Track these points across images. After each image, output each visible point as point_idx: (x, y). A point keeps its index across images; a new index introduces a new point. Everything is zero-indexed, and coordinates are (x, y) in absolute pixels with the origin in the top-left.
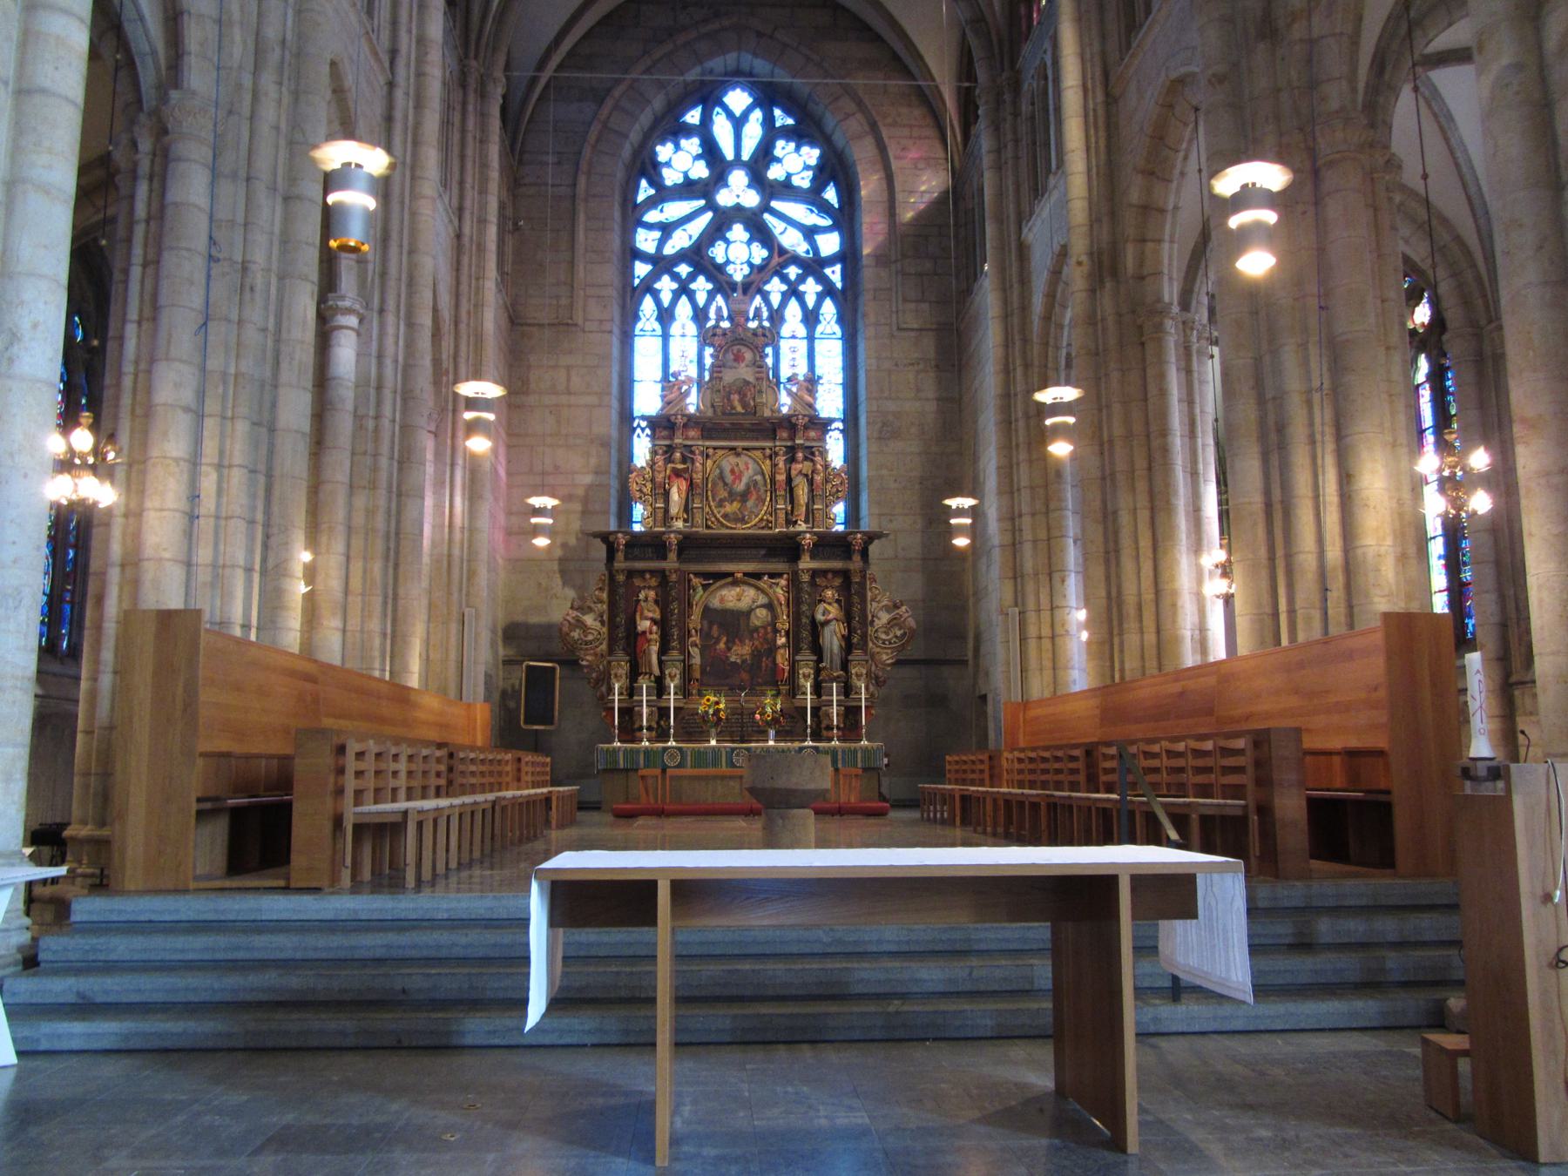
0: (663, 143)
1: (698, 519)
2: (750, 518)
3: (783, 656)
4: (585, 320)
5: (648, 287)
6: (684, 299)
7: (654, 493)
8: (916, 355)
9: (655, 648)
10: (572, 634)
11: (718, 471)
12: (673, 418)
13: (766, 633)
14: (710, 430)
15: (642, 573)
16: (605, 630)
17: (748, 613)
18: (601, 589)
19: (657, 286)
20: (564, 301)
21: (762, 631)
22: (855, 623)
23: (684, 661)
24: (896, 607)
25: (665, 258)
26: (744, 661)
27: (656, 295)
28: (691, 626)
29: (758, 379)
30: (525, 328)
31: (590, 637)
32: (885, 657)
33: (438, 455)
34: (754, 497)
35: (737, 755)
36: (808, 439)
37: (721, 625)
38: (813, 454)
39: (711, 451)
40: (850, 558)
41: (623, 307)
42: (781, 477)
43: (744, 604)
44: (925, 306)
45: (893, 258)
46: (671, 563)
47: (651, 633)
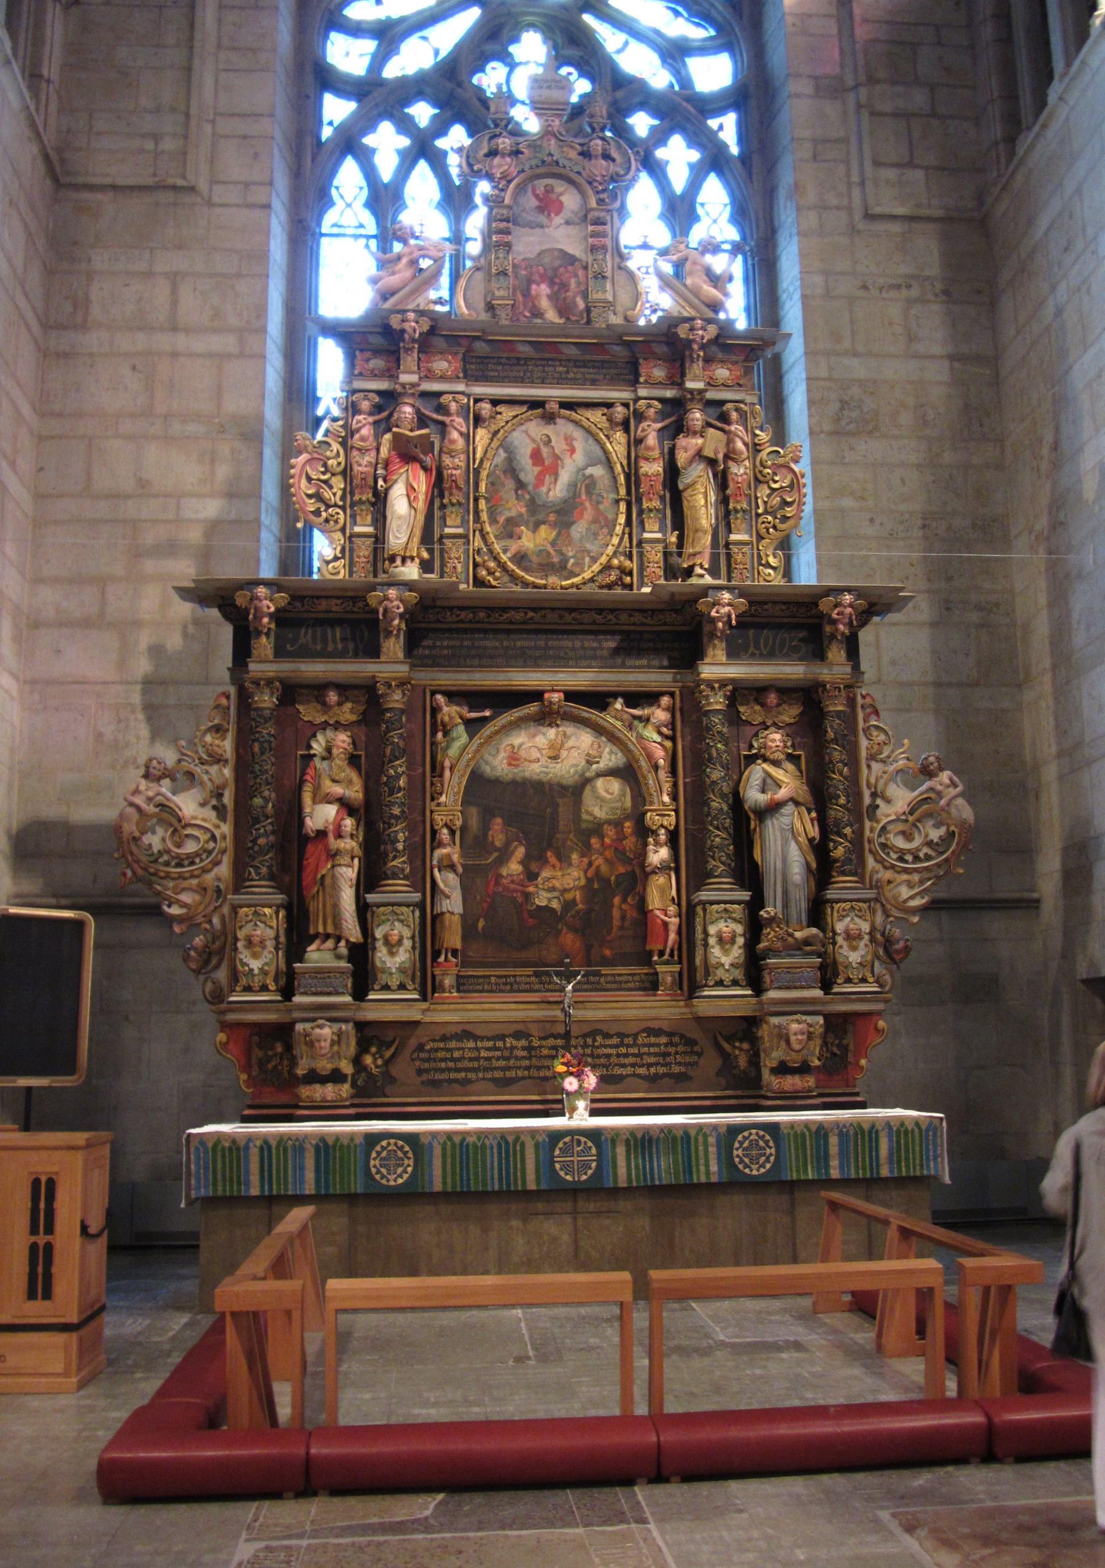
1: (456, 558)
2: (579, 564)
3: (663, 891)
4: (213, 181)
6: (423, 167)
7: (349, 503)
8: (903, 269)
9: (348, 873)
10: (147, 839)
11: (502, 454)
12: (395, 322)
13: (621, 837)
14: (483, 359)
15: (317, 690)
16: (226, 828)
17: (577, 789)
18: (218, 729)
19: (369, 140)
20: (169, 144)
21: (610, 832)
22: (836, 812)
23: (421, 906)
24: (927, 772)
25: (382, 83)
26: (568, 905)
27: (365, 159)
28: (439, 819)
29: (594, 249)
30: (86, 195)
31: (190, 847)
32: (905, 892)
34: (589, 514)
35: (567, 1150)
36: (711, 384)
37: (514, 819)
38: (724, 418)
39: (486, 408)
40: (820, 655)
41: (297, 174)
42: (653, 468)
43: (567, 768)
44: (919, 175)
45: (850, 81)
47: (339, 835)
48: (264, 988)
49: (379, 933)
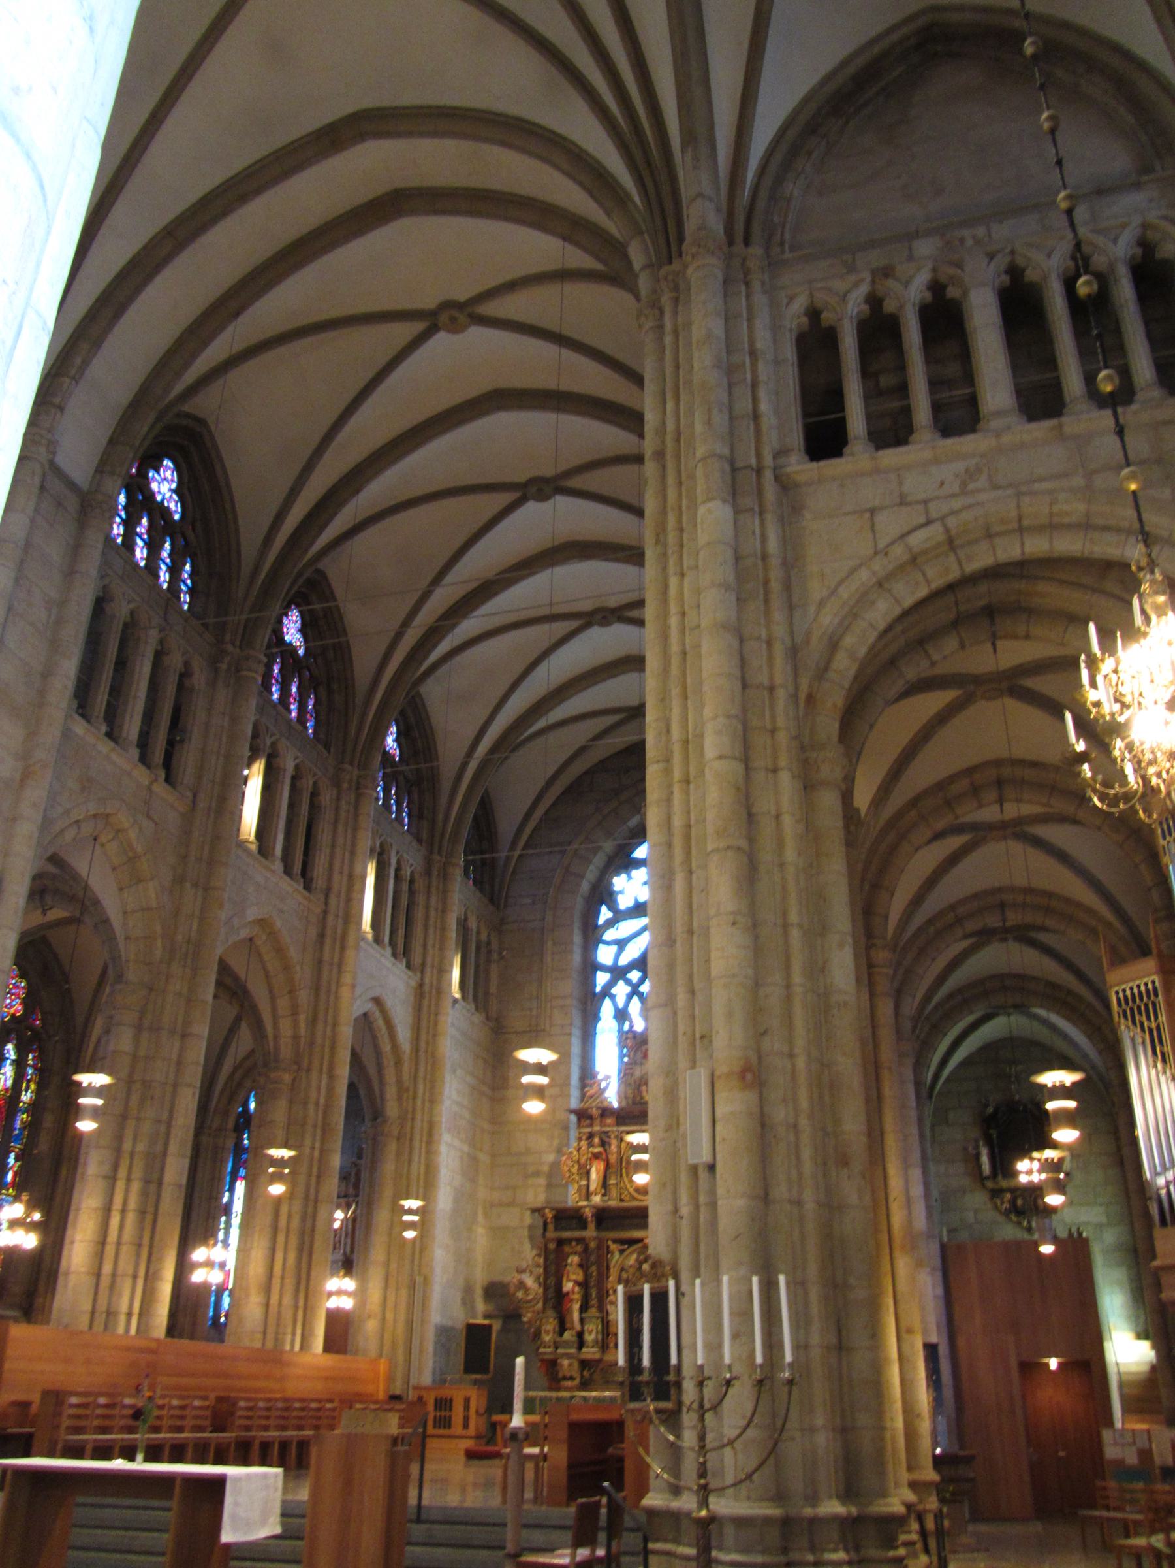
0: (618, 874)
1: (614, 1192)
5: (606, 992)
6: (635, 998)
9: (576, 1307)
15: (569, 1241)
16: (541, 1290)
19: (613, 991)
27: (613, 997)
33: (398, 1154)
46: (590, 1232)
48: (549, 1347)
49: (586, 1327)
